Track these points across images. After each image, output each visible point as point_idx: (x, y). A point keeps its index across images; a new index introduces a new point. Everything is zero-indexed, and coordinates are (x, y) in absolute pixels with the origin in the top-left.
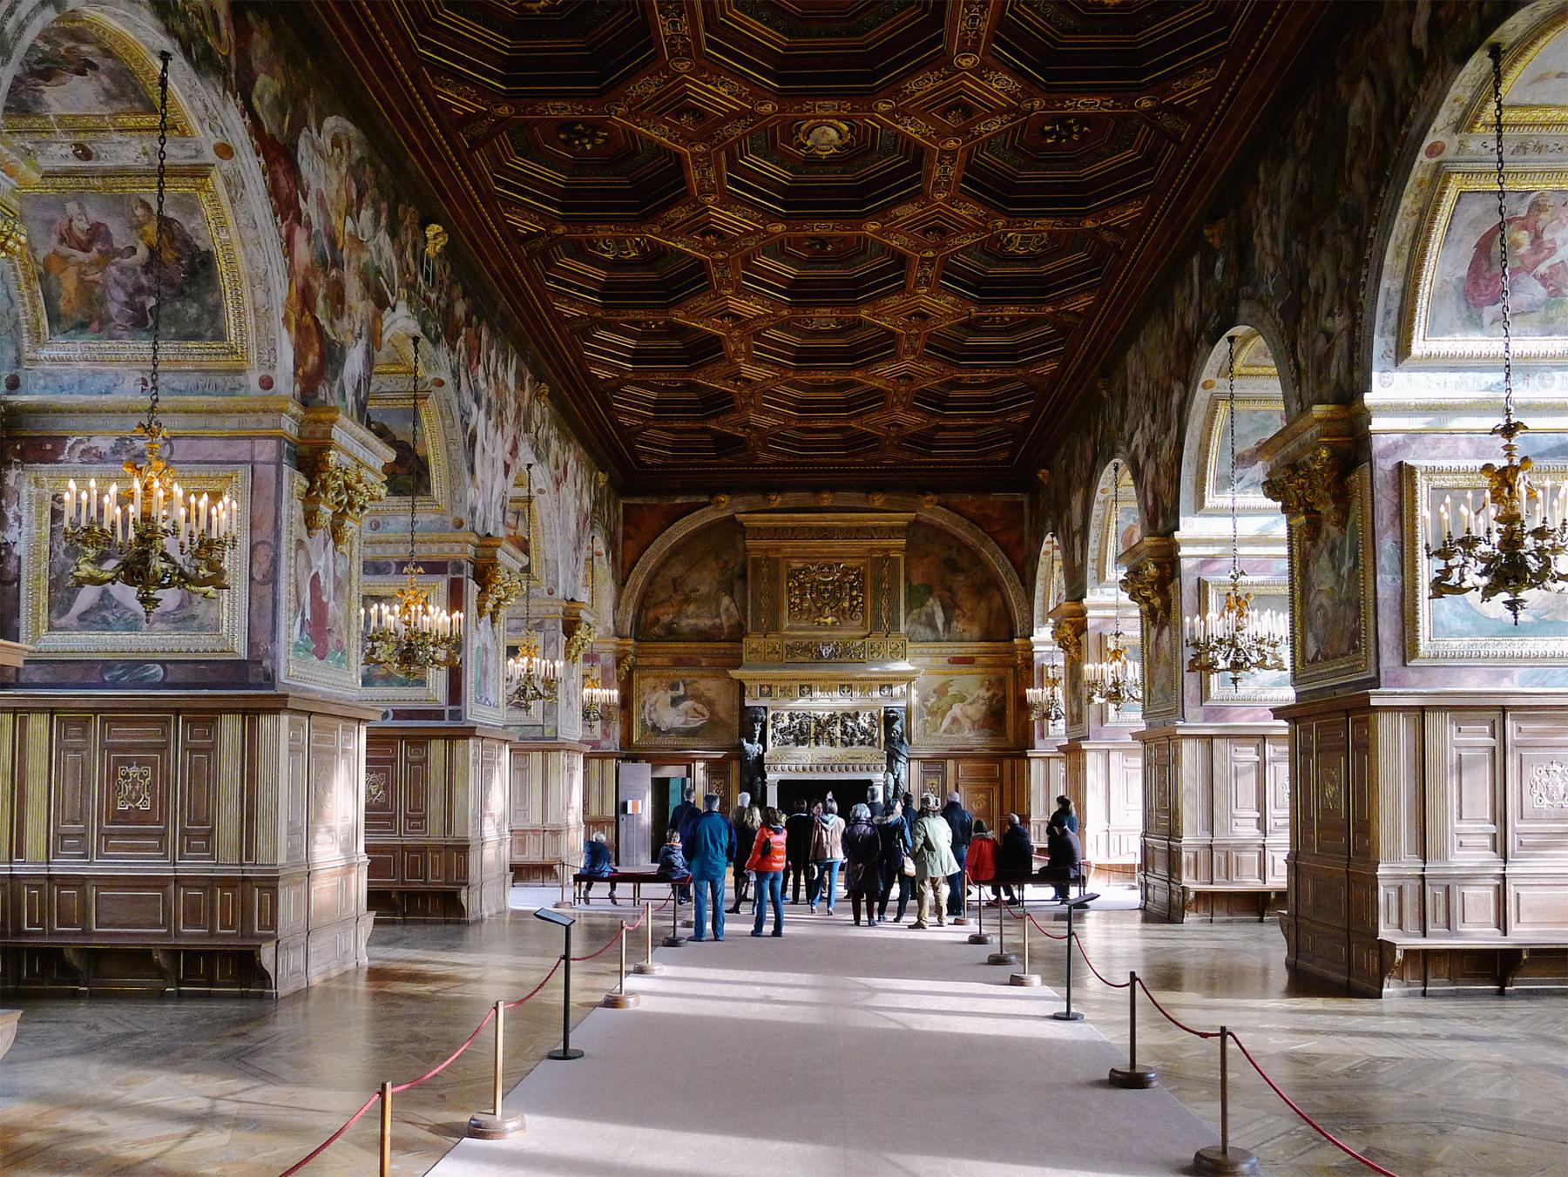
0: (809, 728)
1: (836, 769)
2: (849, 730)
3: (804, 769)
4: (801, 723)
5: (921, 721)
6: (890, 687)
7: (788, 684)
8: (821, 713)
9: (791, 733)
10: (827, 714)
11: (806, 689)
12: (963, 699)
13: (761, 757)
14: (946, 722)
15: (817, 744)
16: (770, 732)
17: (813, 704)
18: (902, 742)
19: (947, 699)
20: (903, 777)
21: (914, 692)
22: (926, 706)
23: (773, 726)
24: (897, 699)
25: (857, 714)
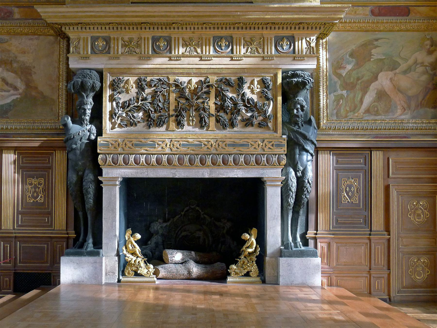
0: (167, 100)
1: (209, 161)
2: (229, 103)
3: (159, 162)
4: (154, 95)
5: (332, 96)
6: (292, 40)
7: (134, 34)
8: (184, 79)
9: (139, 109)
10: (195, 80)
11: (162, 44)
12: (393, 67)
13: (93, 144)
14: (368, 99)
15: (179, 124)
16: (107, 106)
17: (174, 64)
18: (309, 122)
19: (370, 66)
20: (310, 174)
21: (323, 54)
22: (339, 76)
23: (112, 99)
24: (301, 58)
25: (241, 81)
